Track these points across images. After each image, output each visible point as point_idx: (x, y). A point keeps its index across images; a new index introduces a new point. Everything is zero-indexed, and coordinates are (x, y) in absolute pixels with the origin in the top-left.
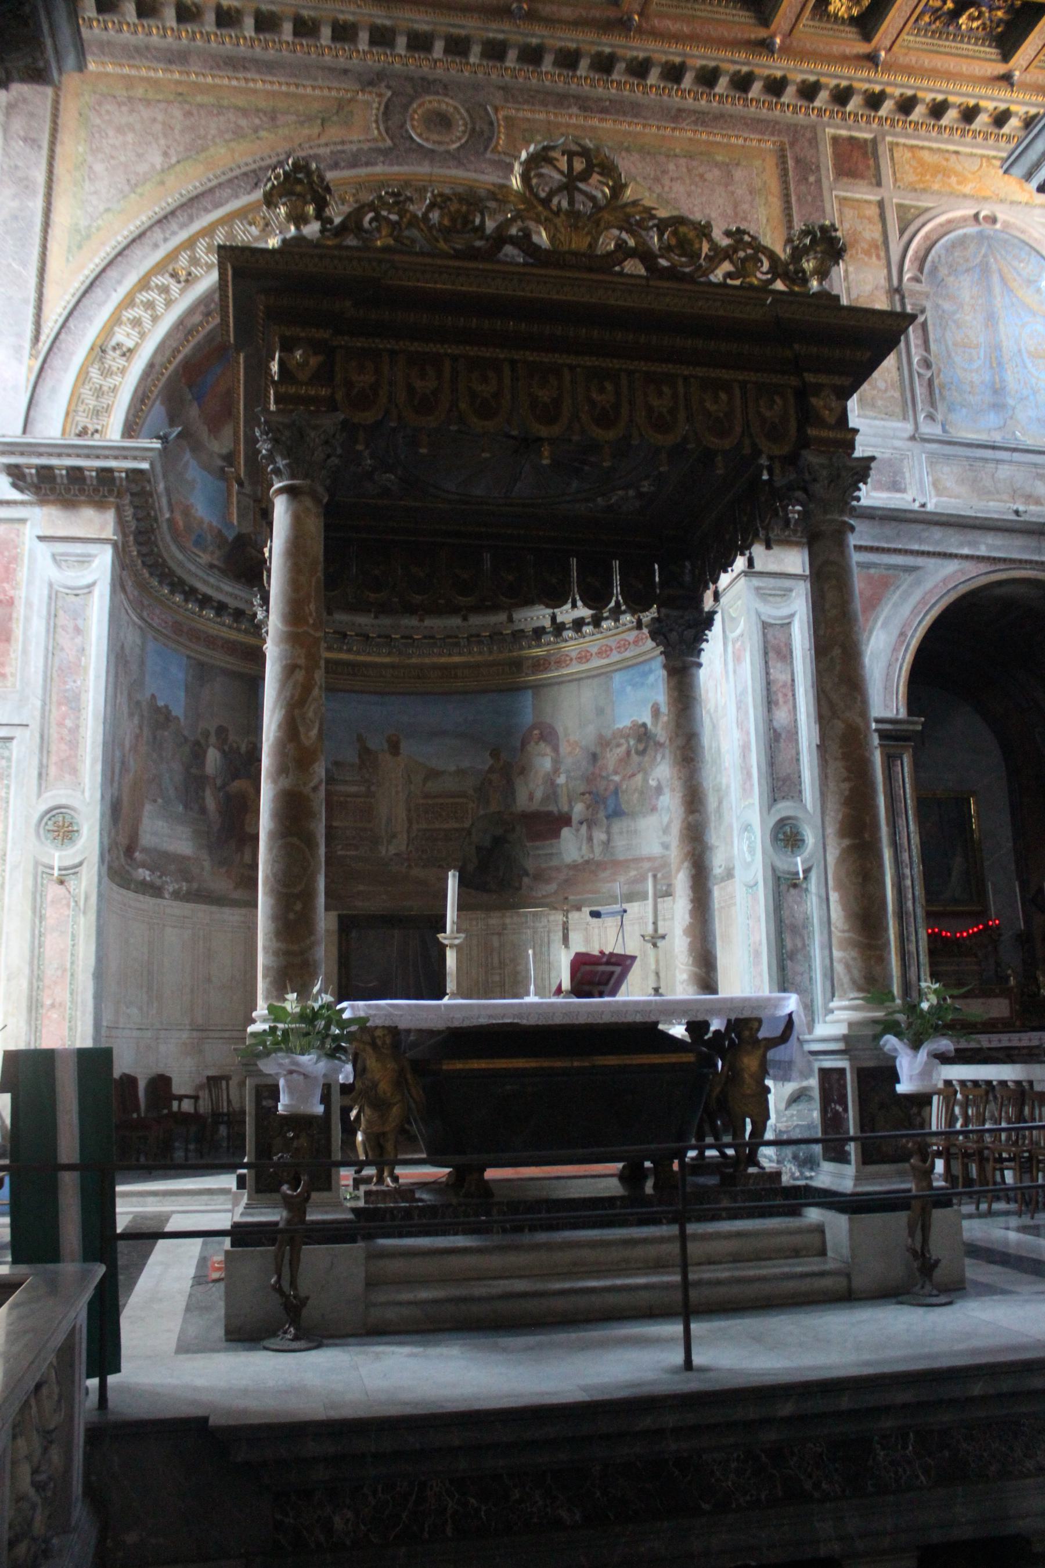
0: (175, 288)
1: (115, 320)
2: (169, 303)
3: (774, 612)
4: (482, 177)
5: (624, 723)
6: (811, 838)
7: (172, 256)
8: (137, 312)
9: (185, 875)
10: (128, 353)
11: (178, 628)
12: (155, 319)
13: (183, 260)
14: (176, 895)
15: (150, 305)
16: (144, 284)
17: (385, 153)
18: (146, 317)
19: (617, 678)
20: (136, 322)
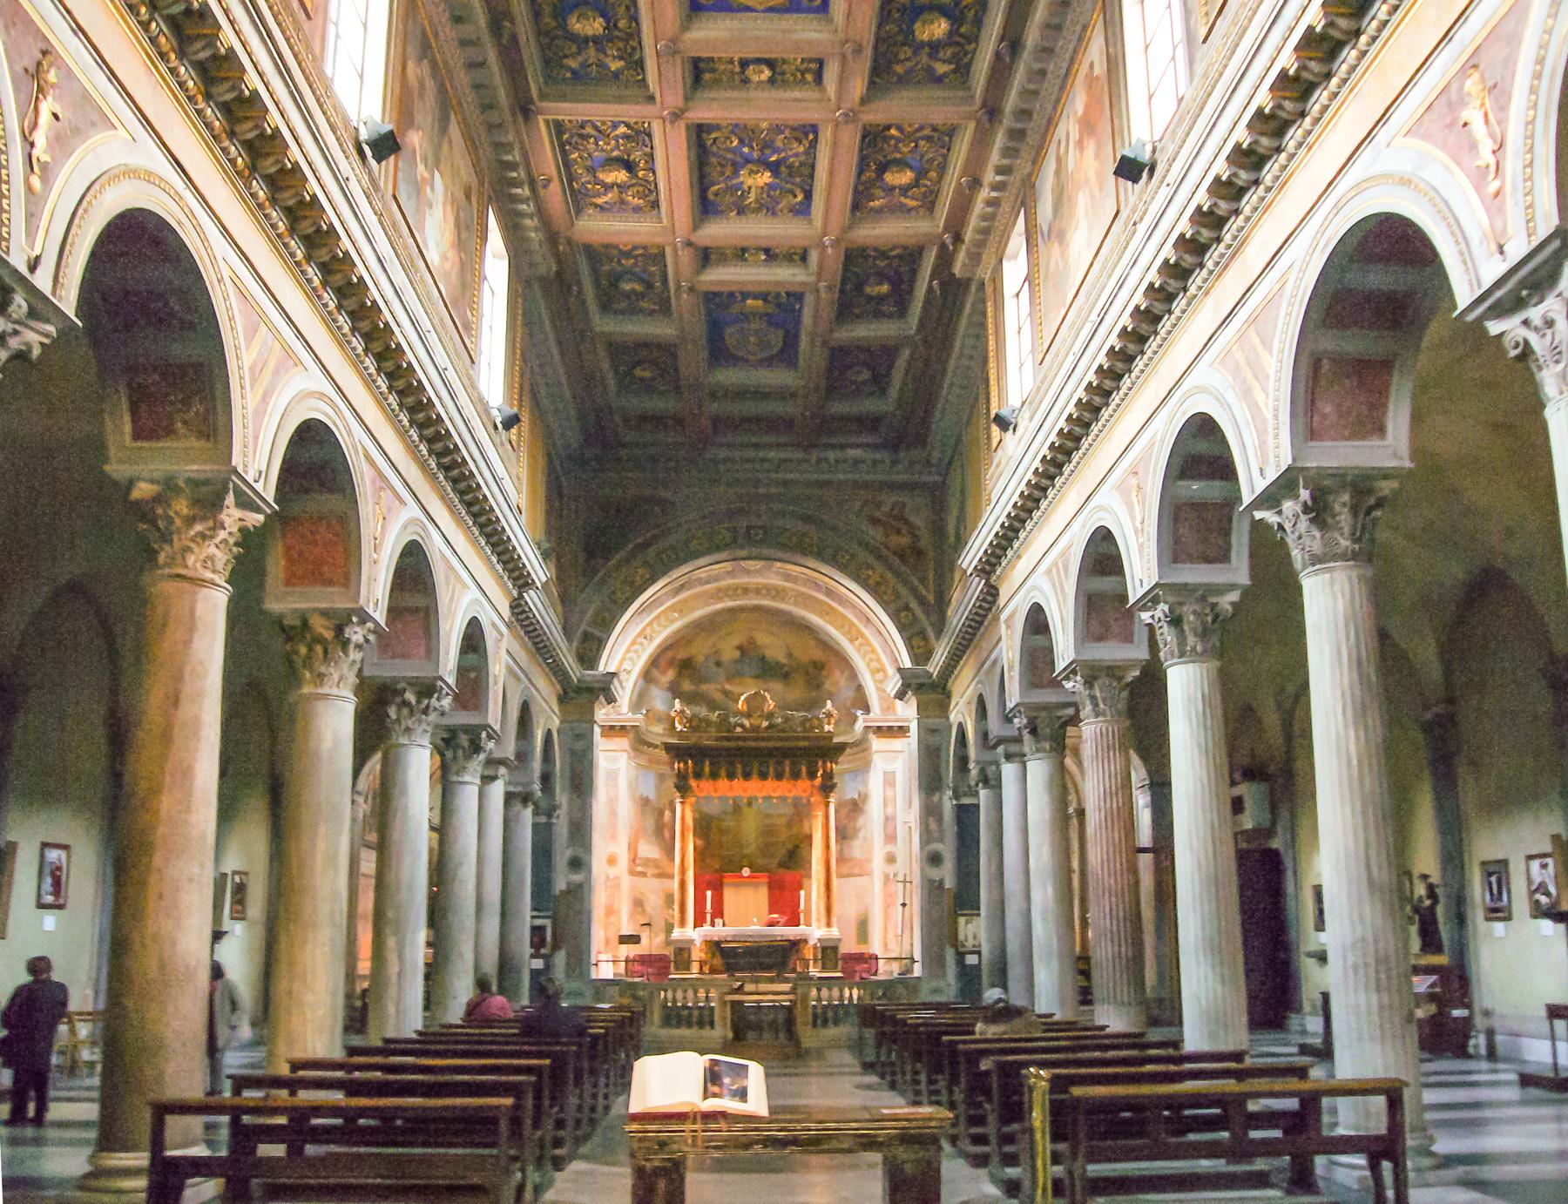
0: (645, 642)
1: (623, 659)
2: (644, 650)
3: (889, 768)
4: (770, 581)
5: (848, 797)
6: (899, 859)
7: (644, 629)
8: (631, 655)
9: (657, 866)
10: (629, 672)
11: (650, 761)
12: (639, 657)
13: (648, 631)
14: (653, 876)
15: (636, 651)
16: (634, 643)
17: (728, 573)
18: (635, 656)
19: (847, 777)
20: (631, 659)
